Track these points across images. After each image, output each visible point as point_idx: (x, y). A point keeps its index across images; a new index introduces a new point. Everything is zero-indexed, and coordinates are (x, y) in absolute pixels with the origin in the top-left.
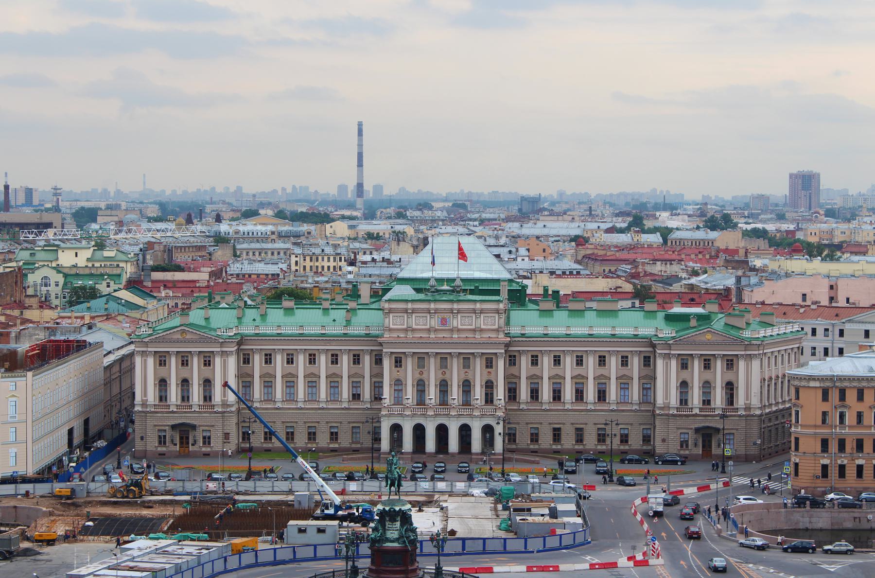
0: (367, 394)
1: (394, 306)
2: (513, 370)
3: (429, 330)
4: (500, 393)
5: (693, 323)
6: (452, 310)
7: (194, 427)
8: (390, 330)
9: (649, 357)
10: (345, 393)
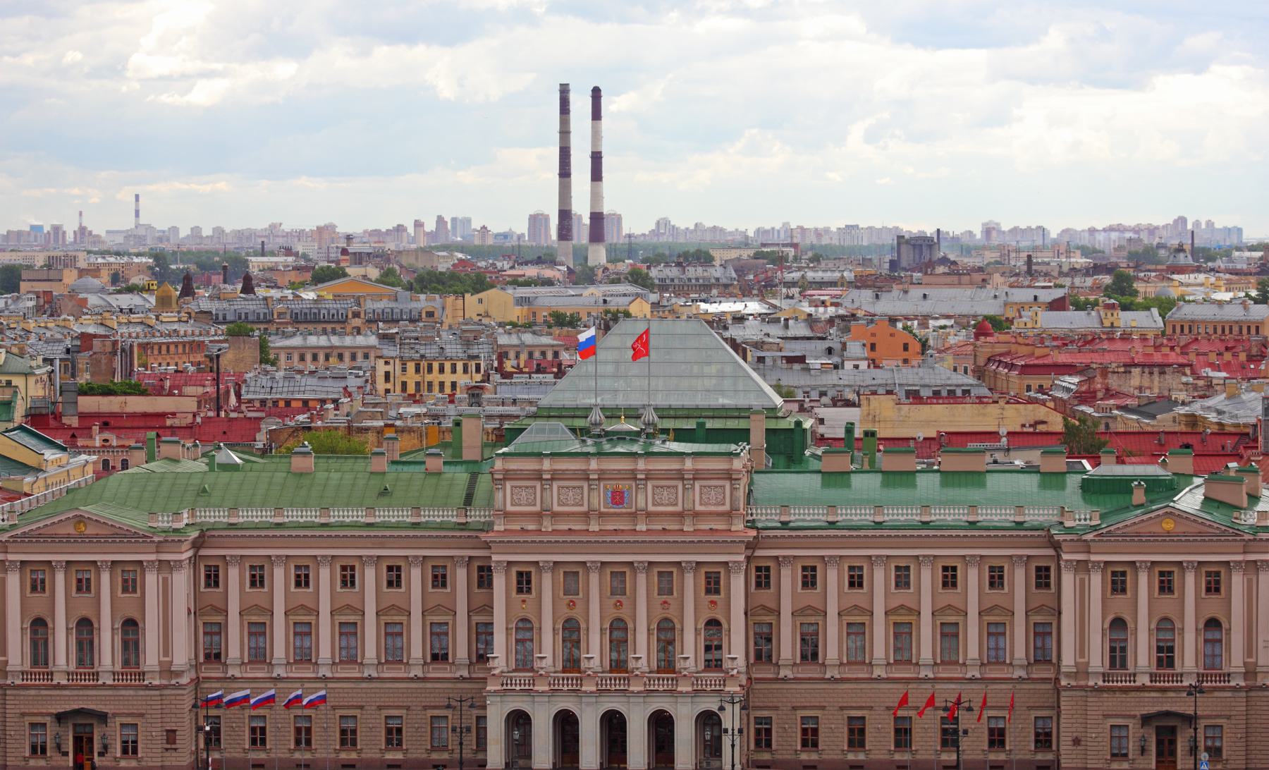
0: (461, 649)
1: (514, 465)
2: (765, 597)
3: (586, 516)
4: (737, 649)
5: (1139, 496)
6: (634, 472)
7: (103, 717)
8: (507, 515)
9: (1048, 569)
10: (417, 648)
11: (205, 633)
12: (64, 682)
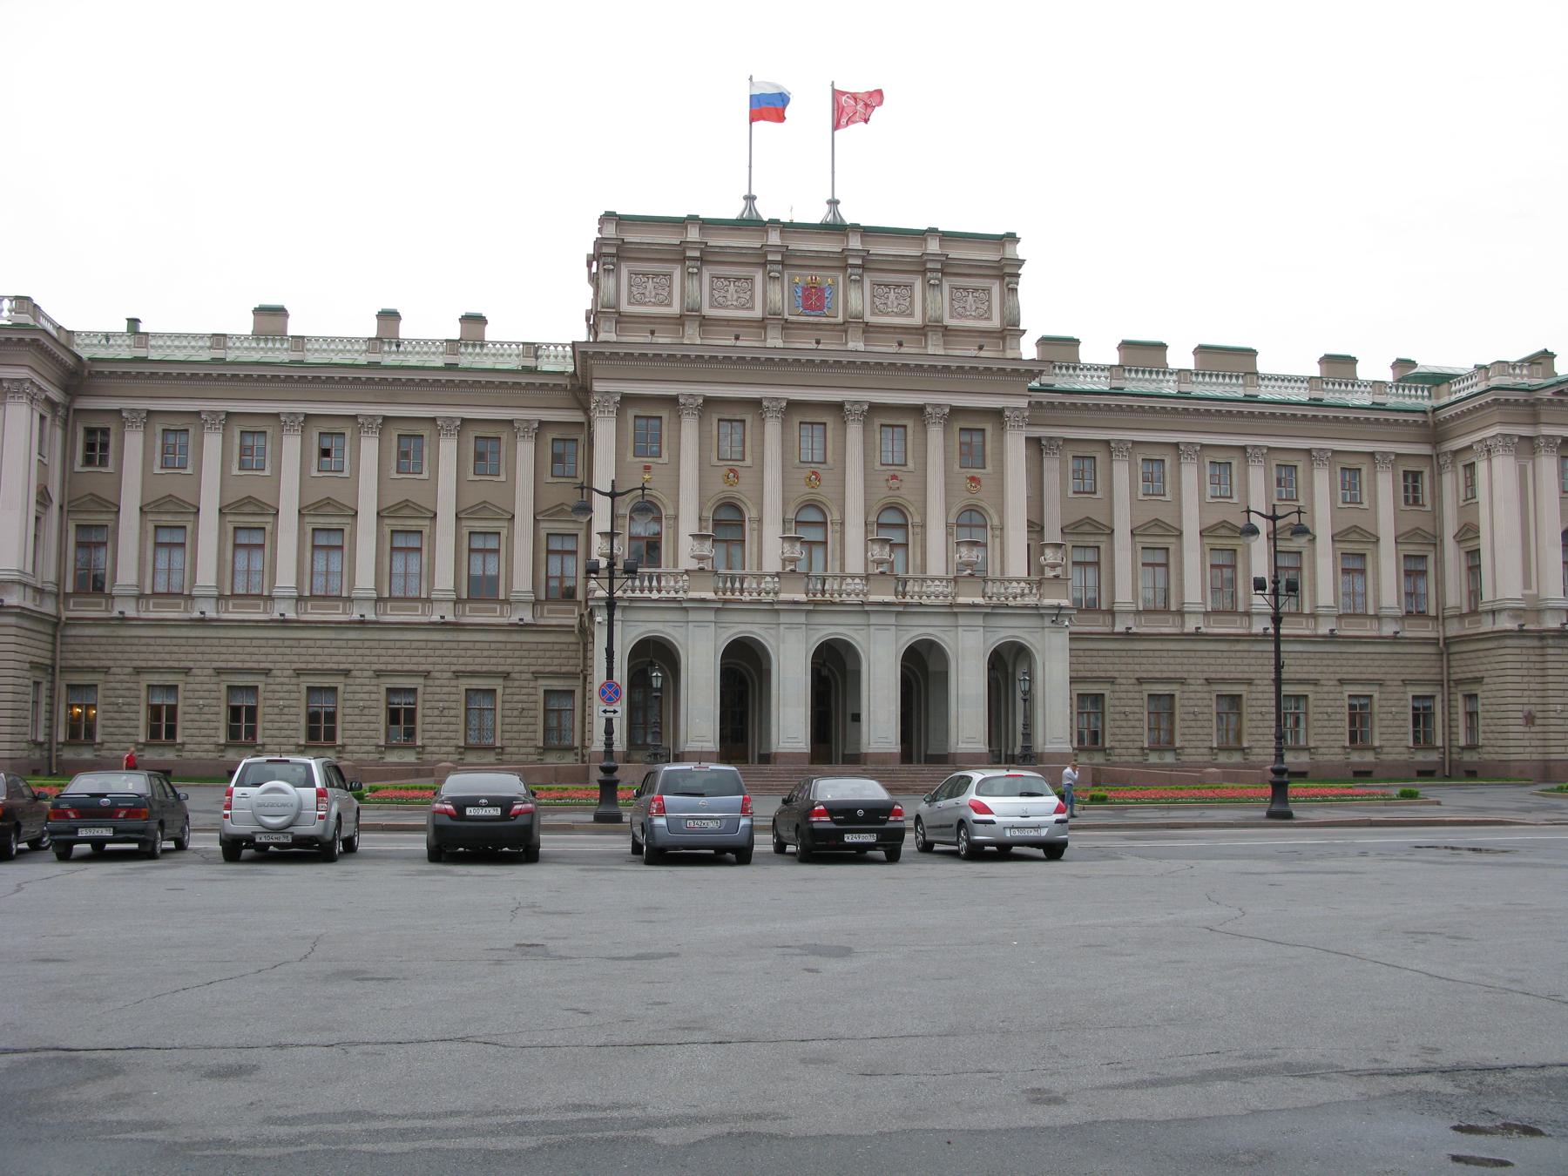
6: (844, 254)
11: (79, 545)
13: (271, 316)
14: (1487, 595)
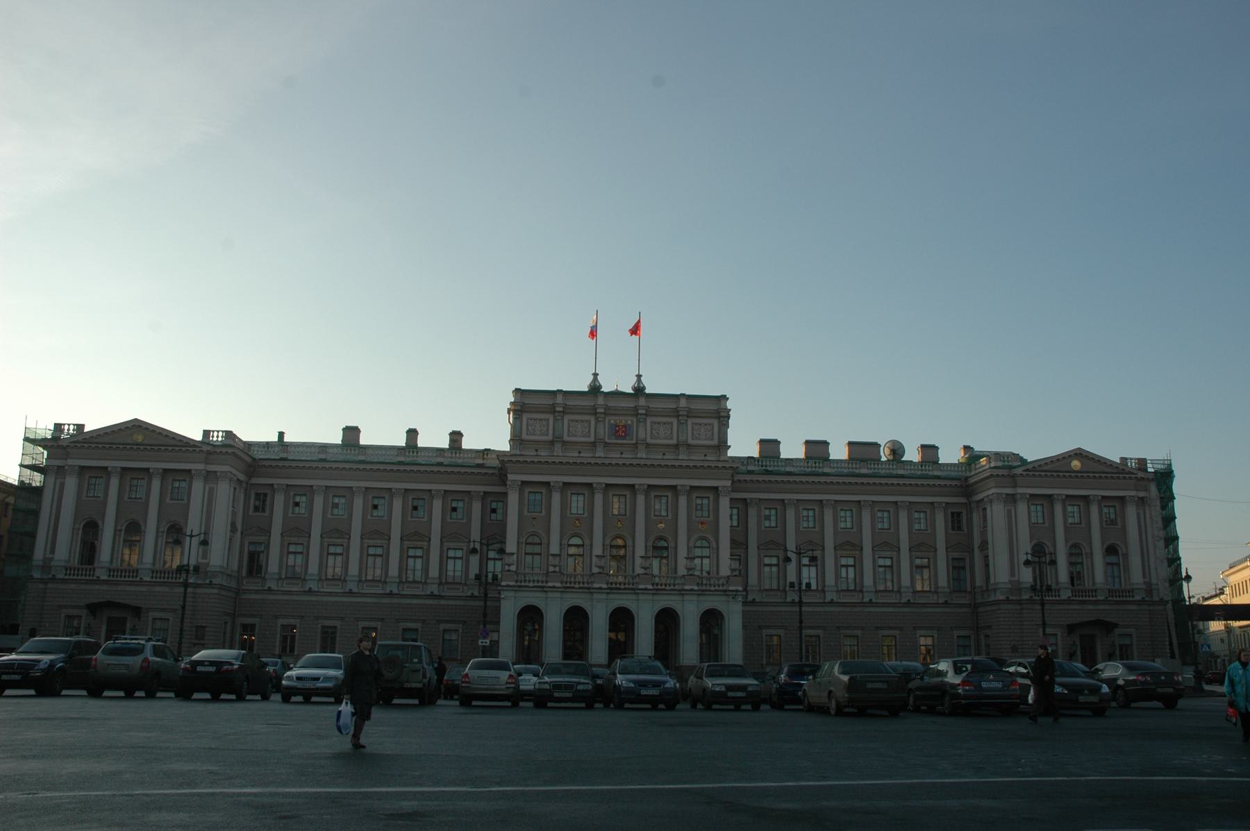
12: (104, 577)
13: (351, 433)
14: (992, 581)
